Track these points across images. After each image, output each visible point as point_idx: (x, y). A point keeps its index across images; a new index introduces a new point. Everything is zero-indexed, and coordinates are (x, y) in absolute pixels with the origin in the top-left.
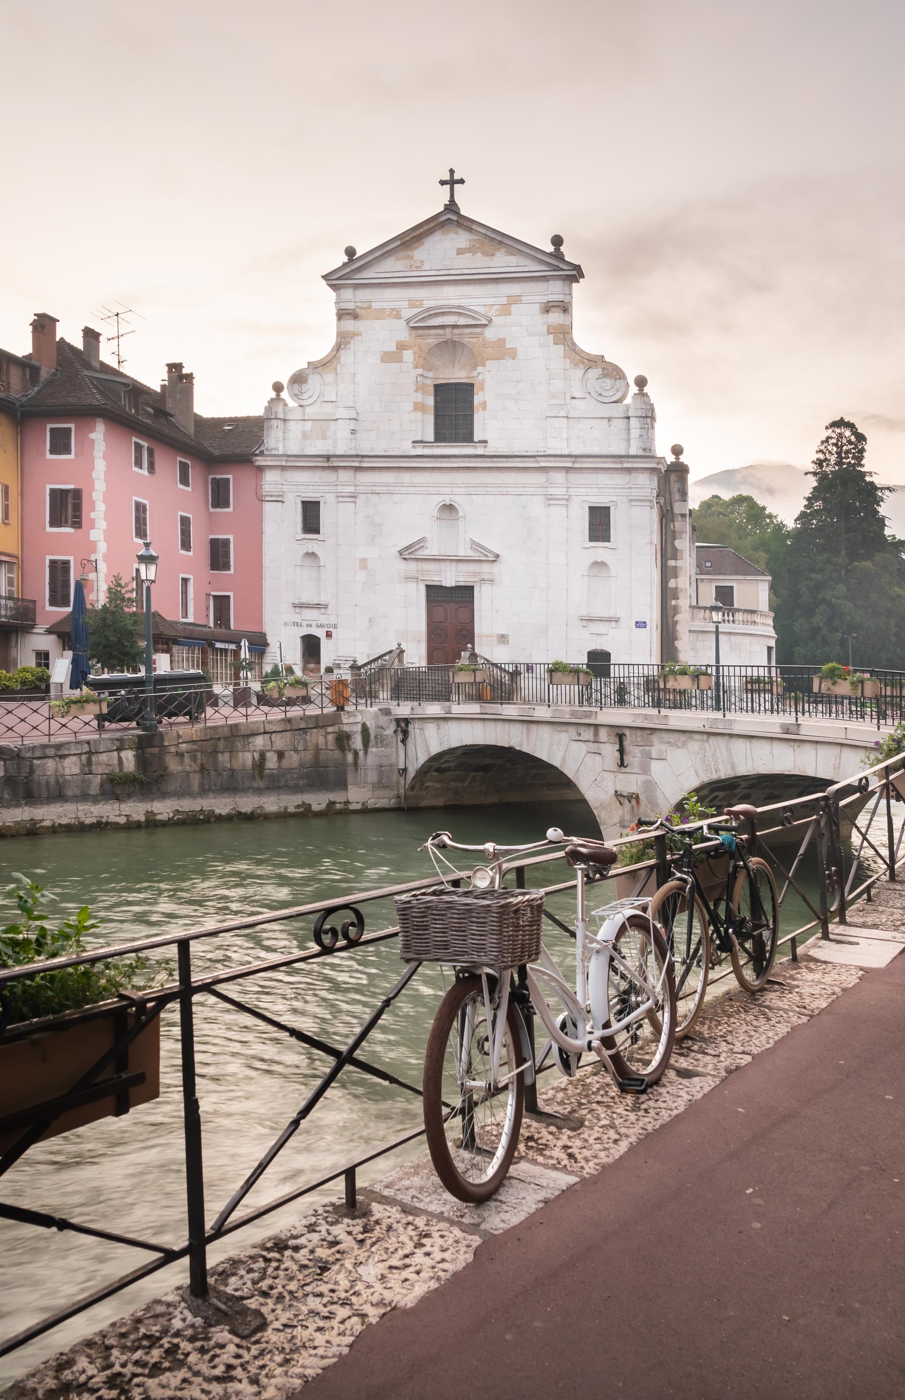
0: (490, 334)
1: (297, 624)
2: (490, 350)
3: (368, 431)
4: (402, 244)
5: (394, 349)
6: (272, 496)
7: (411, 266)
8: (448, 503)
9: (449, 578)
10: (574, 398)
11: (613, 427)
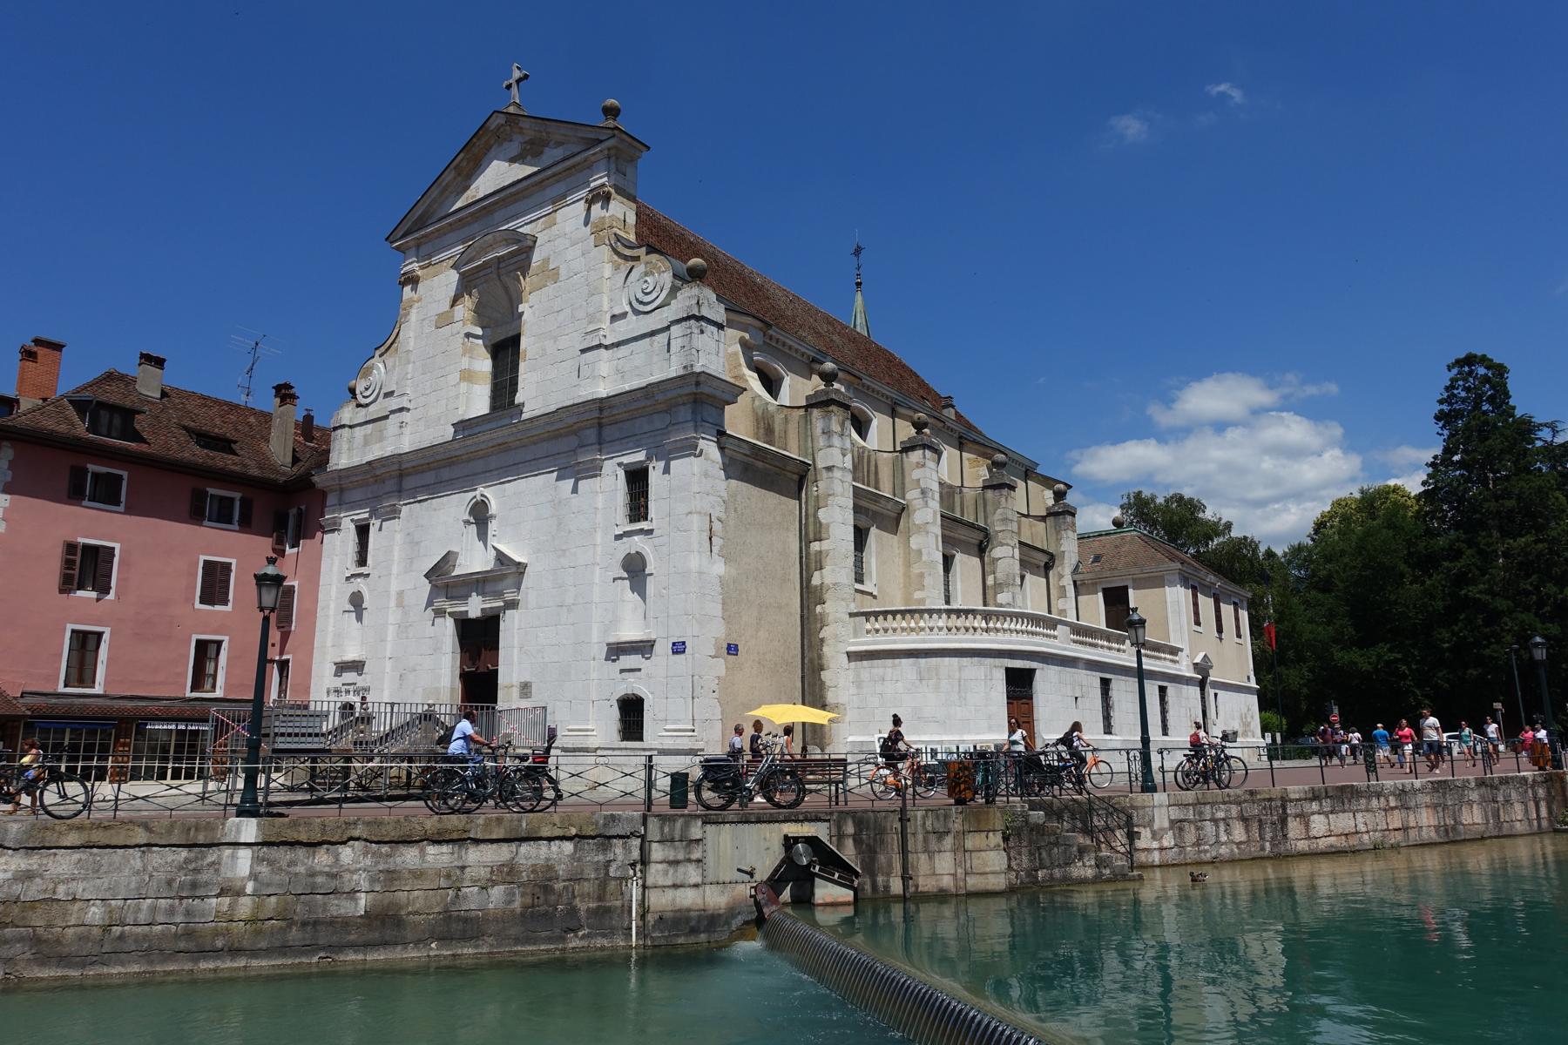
0: (537, 257)
1: (337, 691)
5: (447, 308)
8: (479, 498)
9: (475, 607)
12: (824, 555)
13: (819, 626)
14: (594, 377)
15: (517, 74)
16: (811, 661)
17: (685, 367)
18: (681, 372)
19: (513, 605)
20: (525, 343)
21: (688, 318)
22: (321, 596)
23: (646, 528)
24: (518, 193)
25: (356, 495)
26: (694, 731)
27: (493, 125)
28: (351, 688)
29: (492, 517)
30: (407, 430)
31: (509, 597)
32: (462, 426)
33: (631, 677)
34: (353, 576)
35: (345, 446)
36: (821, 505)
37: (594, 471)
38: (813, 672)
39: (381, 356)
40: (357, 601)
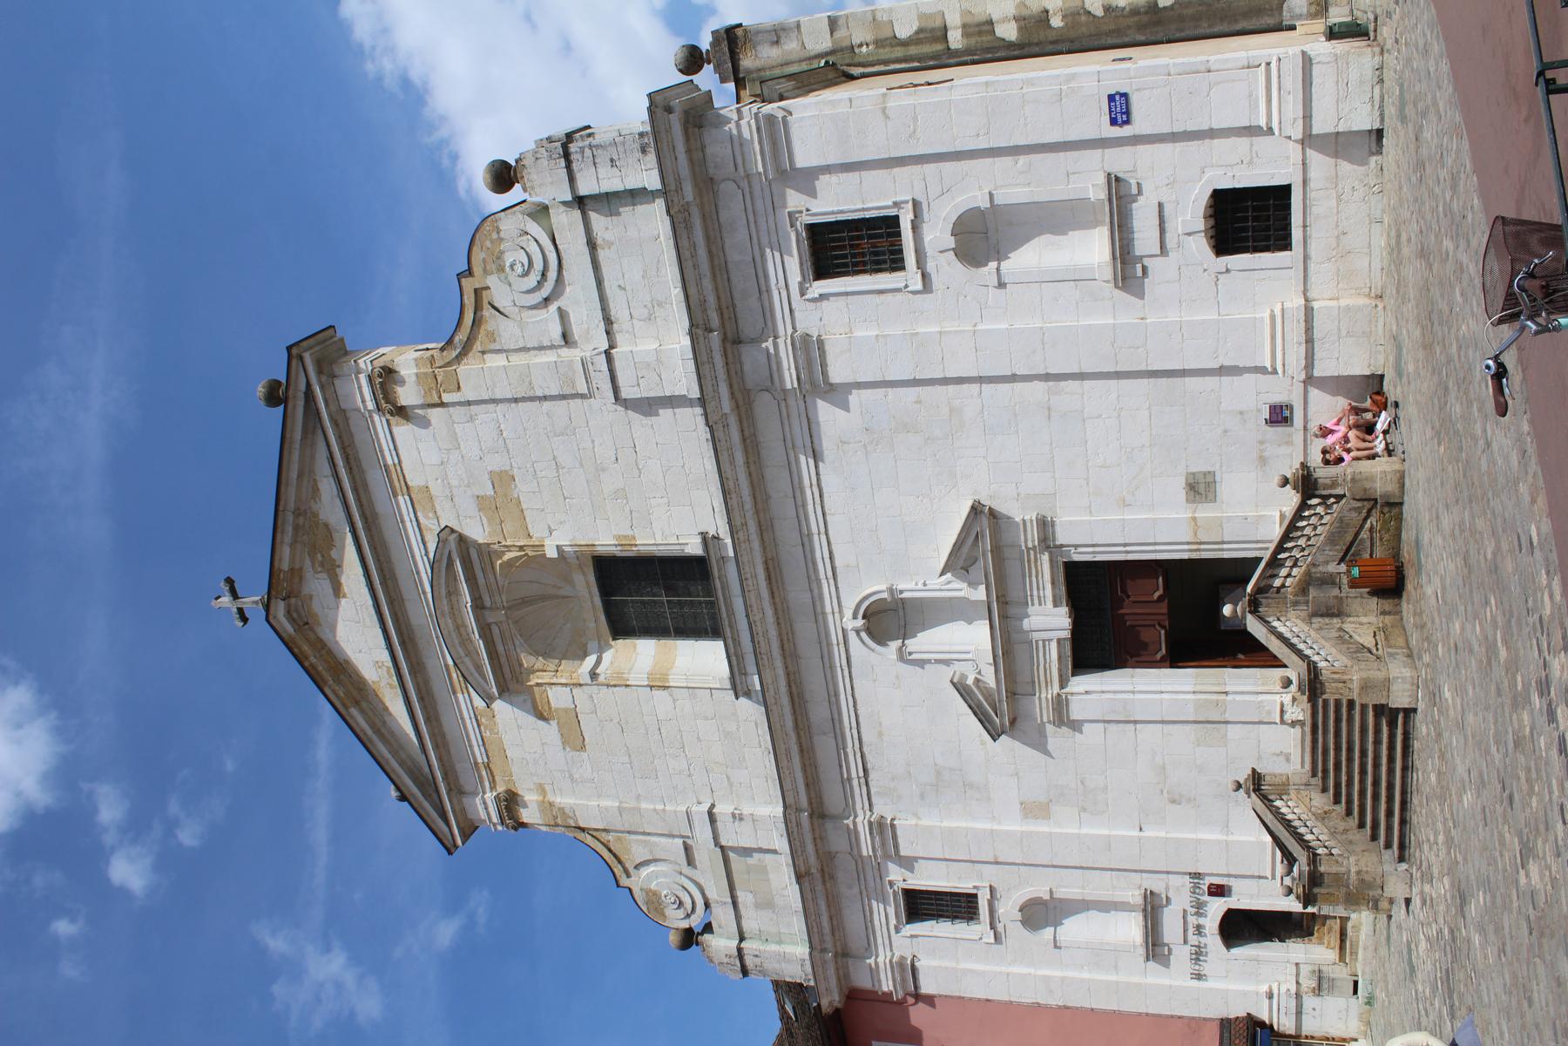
0: (477, 531)
1: (1198, 954)
2: (508, 527)
3: (731, 785)
4: (357, 703)
6: (904, 980)
7: (391, 686)
8: (860, 622)
10: (564, 336)
11: (609, 236)
12: (969, 20)
13: (1083, 18)
14: (658, 360)
15: (226, 600)
16: (1141, 27)
17: (644, 150)
18: (651, 158)
19: (1045, 525)
20: (606, 541)
21: (567, 155)
22: (1028, 997)
23: (911, 216)
24: (381, 570)
25: (853, 920)
26: (1268, 64)
27: (288, 628)
28: (1192, 920)
29: (891, 590)
30: (746, 810)
31: (1033, 537)
32: (738, 686)
33: (1176, 226)
34: (993, 927)
35: (773, 947)
36: (889, 34)
37: (811, 350)
38: (1159, 23)
39: (628, 875)
40: (1040, 914)
